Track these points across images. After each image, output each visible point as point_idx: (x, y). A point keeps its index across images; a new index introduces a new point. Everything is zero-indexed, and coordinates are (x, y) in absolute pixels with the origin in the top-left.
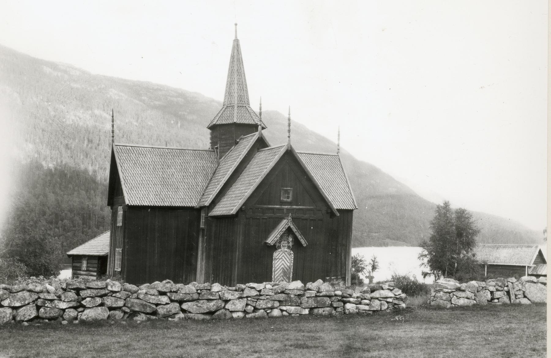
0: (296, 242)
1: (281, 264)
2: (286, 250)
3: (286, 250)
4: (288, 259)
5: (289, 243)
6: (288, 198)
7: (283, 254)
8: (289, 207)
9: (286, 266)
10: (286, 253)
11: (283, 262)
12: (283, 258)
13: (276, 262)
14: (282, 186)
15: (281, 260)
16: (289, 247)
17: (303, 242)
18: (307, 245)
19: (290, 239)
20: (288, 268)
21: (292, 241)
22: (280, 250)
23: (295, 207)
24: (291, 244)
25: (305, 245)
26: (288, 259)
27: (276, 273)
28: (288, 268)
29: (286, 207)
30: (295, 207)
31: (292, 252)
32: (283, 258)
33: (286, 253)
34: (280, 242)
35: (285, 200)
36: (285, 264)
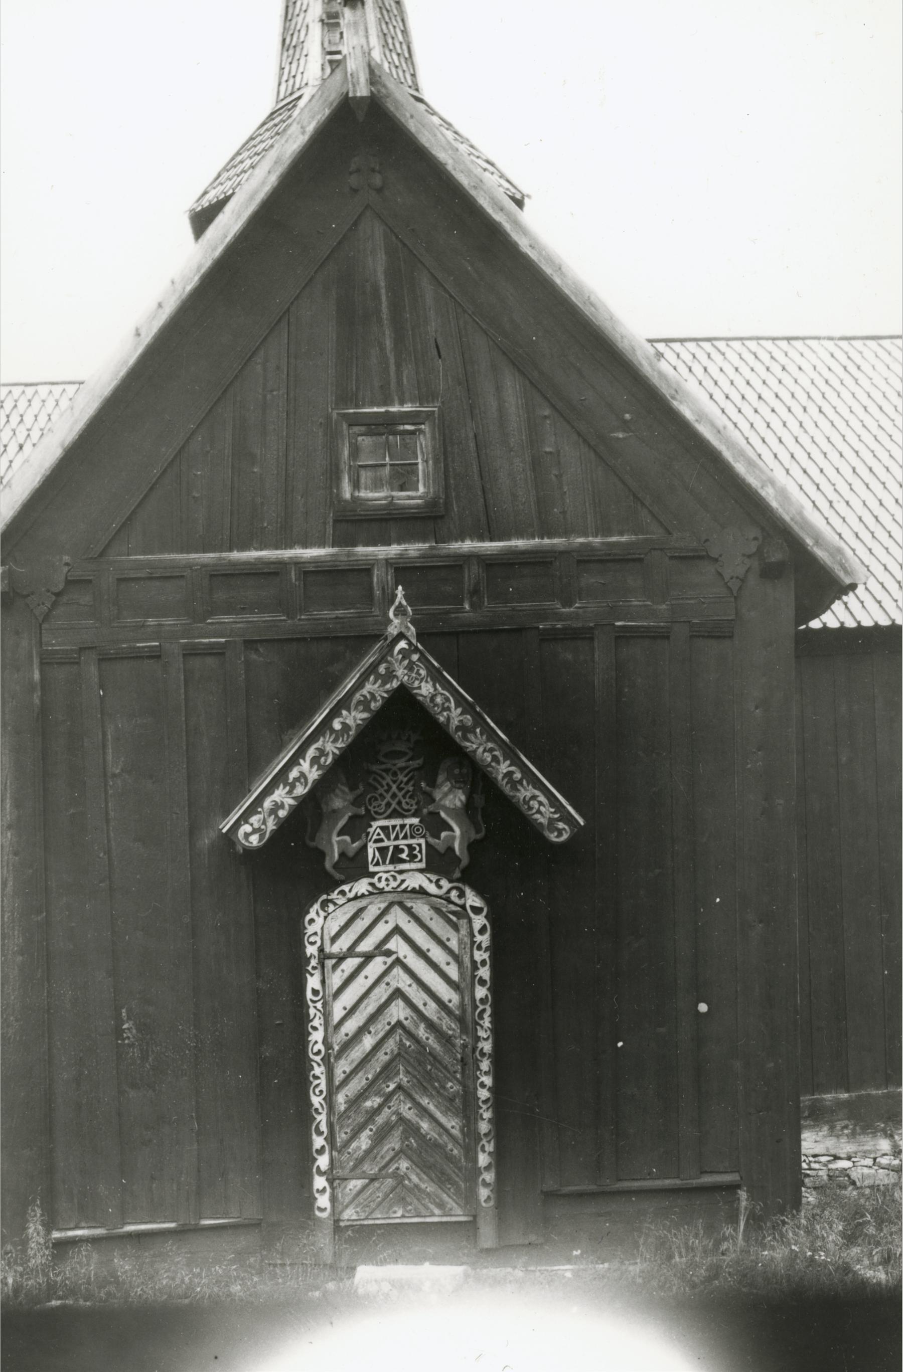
0: (492, 808)
1: (381, 994)
3: (416, 880)
4: (437, 954)
5: (434, 825)
6: (404, 477)
7: (398, 917)
8: (414, 549)
9: (431, 1010)
10: (422, 909)
11: (399, 979)
12: (397, 945)
14: (346, 398)
16: (439, 863)
17: (547, 808)
18: (578, 834)
19: (451, 798)
20: (448, 1025)
21: (468, 806)
22: (362, 886)
23: (468, 545)
24: (457, 836)
26: (437, 954)
27: (342, 1068)
28: (448, 1025)
29: (394, 550)
30: (468, 545)
31: (472, 899)
32: (397, 945)
34: (357, 827)
35: (374, 496)
36: (418, 997)
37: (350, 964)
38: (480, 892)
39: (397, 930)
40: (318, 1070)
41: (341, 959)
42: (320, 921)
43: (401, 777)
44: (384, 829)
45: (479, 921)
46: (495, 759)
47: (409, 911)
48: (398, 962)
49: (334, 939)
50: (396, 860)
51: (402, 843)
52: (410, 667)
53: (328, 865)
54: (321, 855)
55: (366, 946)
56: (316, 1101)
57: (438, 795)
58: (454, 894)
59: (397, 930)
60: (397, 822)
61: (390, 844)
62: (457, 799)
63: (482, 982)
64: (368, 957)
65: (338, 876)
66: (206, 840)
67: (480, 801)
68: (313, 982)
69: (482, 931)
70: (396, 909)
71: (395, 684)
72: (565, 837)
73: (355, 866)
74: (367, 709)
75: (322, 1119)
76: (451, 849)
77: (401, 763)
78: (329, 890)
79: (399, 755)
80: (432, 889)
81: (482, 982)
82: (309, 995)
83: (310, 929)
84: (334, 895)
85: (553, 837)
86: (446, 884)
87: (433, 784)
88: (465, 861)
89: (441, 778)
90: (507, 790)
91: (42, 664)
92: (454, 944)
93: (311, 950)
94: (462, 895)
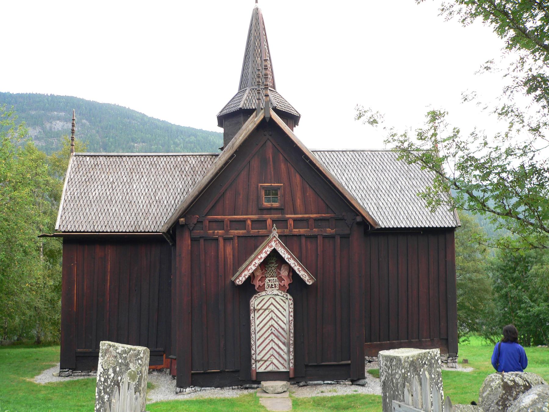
1: (268, 318)
2: (276, 292)
3: (276, 292)
5: (281, 279)
7: (272, 300)
12: (272, 307)
13: (257, 315)
15: (267, 312)
16: (281, 288)
19: (284, 273)
22: (263, 293)
25: (310, 283)
31: (289, 297)
32: (272, 307)
33: (277, 298)
34: (263, 279)
37: (261, 312)
38: (291, 295)
39: (272, 303)
40: (253, 336)
41: (259, 310)
42: (254, 301)
43: (273, 268)
44: (269, 280)
45: (291, 302)
46: (295, 265)
47: (274, 299)
48: (272, 311)
49: (257, 305)
50: (272, 287)
51: (273, 283)
52: (276, 244)
53: (256, 288)
54: (254, 286)
55: (265, 307)
56: (252, 342)
57: (281, 273)
58: (285, 296)
59: (272, 303)
60: (272, 278)
61: (270, 284)
62: (286, 273)
63: (291, 316)
64: (265, 310)
65: (258, 291)
66: (228, 282)
67: (291, 274)
68: (252, 315)
69: (291, 304)
70: (272, 299)
71: (273, 248)
72: (311, 283)
73: (262, 288)
74: (266, 253)
75: (254, 347)
76: (284, 285)
77: (273, 265)
78: (255, 294)
79: (273, 263)
80: (280, 294)
81: (291, 316)
82: (251, 318)
83: (252, 303)
84: (257, 295)
85: (308, 283)
86: (283, 293)
87: (280, 270)
88: (288, 288)
89: (282, 269)
90: (298, 273)
91: (191, 240)
92: (285, 307)
93: (252, 308)
94: (287, 296)
